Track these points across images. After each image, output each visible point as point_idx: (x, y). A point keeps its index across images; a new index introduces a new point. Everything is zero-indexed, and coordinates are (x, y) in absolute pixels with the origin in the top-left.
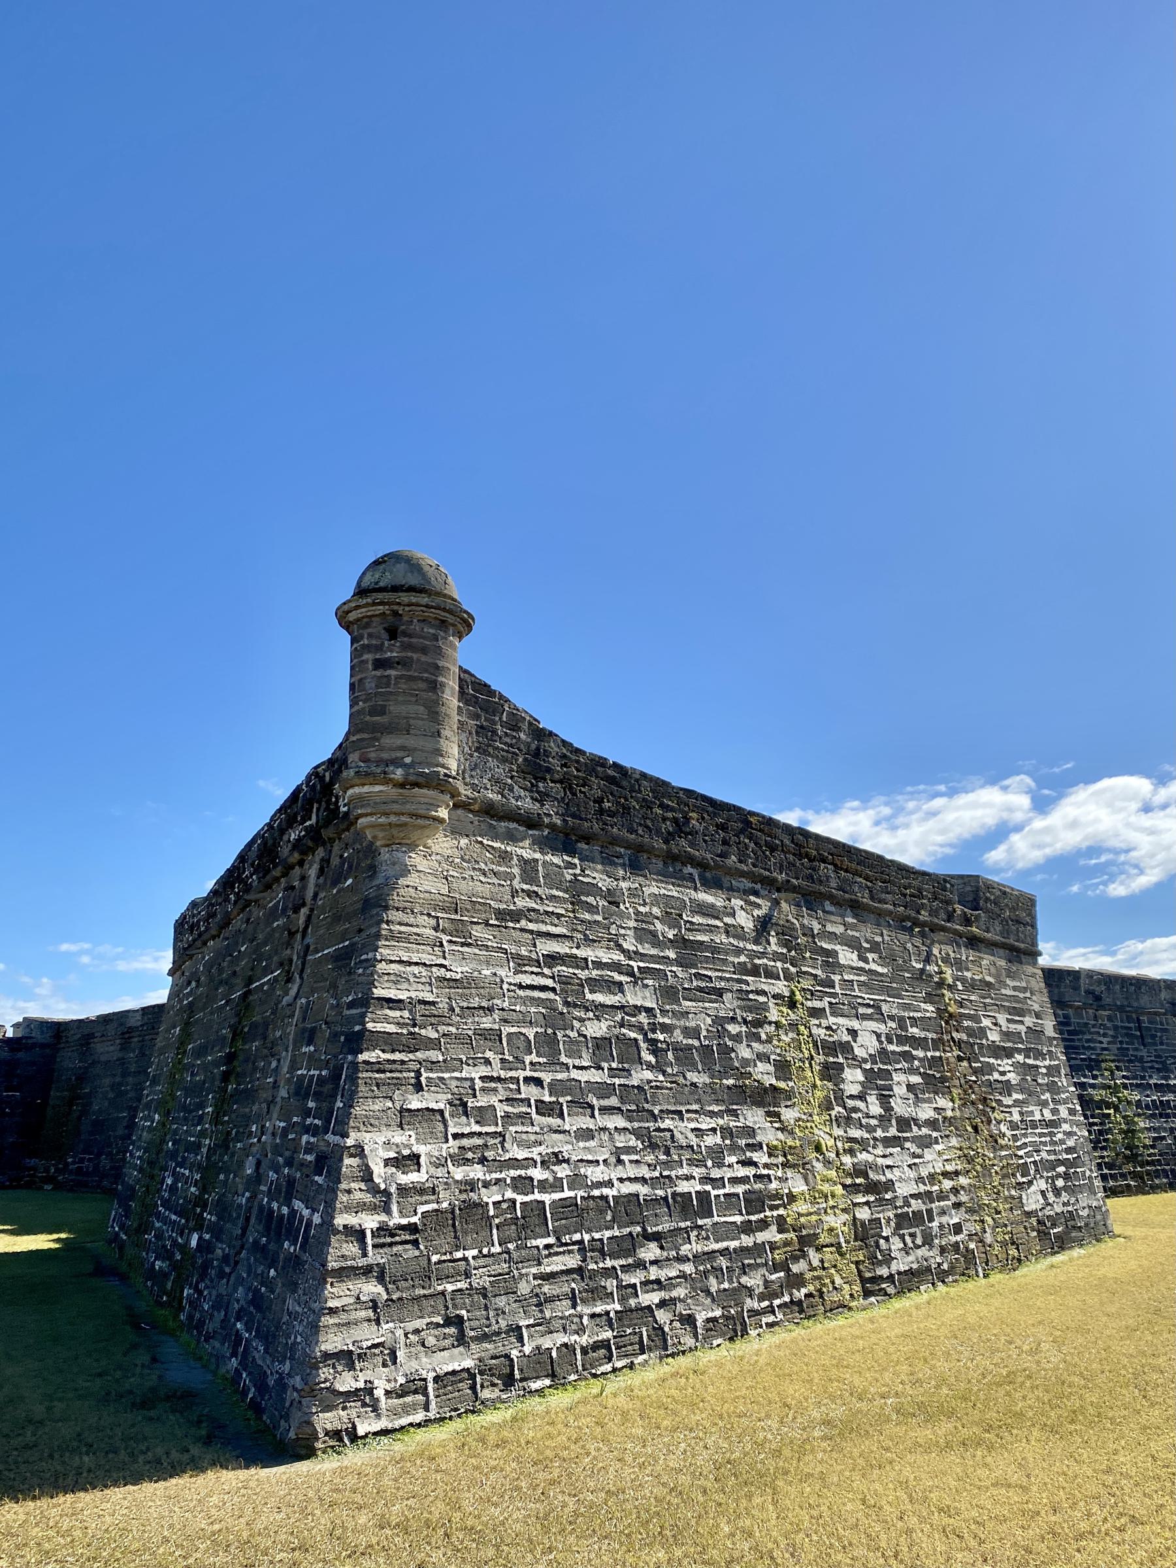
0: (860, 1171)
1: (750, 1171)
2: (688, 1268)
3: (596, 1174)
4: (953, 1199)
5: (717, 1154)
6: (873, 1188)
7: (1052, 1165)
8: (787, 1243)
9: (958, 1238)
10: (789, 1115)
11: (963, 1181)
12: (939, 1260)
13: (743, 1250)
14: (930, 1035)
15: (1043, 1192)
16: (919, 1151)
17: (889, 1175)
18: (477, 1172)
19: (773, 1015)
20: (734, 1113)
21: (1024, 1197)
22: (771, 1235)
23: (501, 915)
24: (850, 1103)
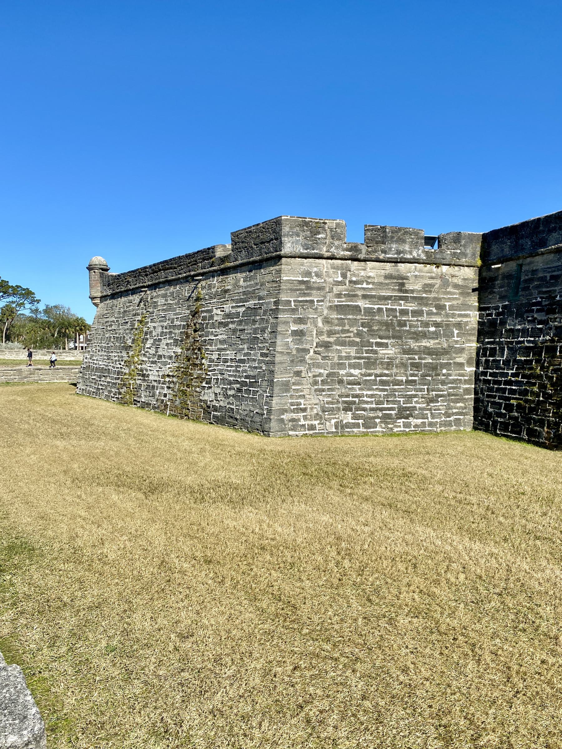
0: (142, 370)
1: (119, 366)
2: (106, 384)
3: (100, 363)
4: (167, 385)
5: (116, 361)
6: (143, 375)
7: (230, 383)
8: (121, 384)
9: (164, 398)
10: (131, 353)
11: (175, 380)
12: (155, 403)
13: (113, 383)
14: (182, 323)
15: (216, 394)
16: (162, 366)
17: (150, 373)
18: (91, 361)
19: (136, 327)
20: (121, 352)
21: (203, 393)
22: (119, 381)
23: (103, 315)
24: (146, 350)
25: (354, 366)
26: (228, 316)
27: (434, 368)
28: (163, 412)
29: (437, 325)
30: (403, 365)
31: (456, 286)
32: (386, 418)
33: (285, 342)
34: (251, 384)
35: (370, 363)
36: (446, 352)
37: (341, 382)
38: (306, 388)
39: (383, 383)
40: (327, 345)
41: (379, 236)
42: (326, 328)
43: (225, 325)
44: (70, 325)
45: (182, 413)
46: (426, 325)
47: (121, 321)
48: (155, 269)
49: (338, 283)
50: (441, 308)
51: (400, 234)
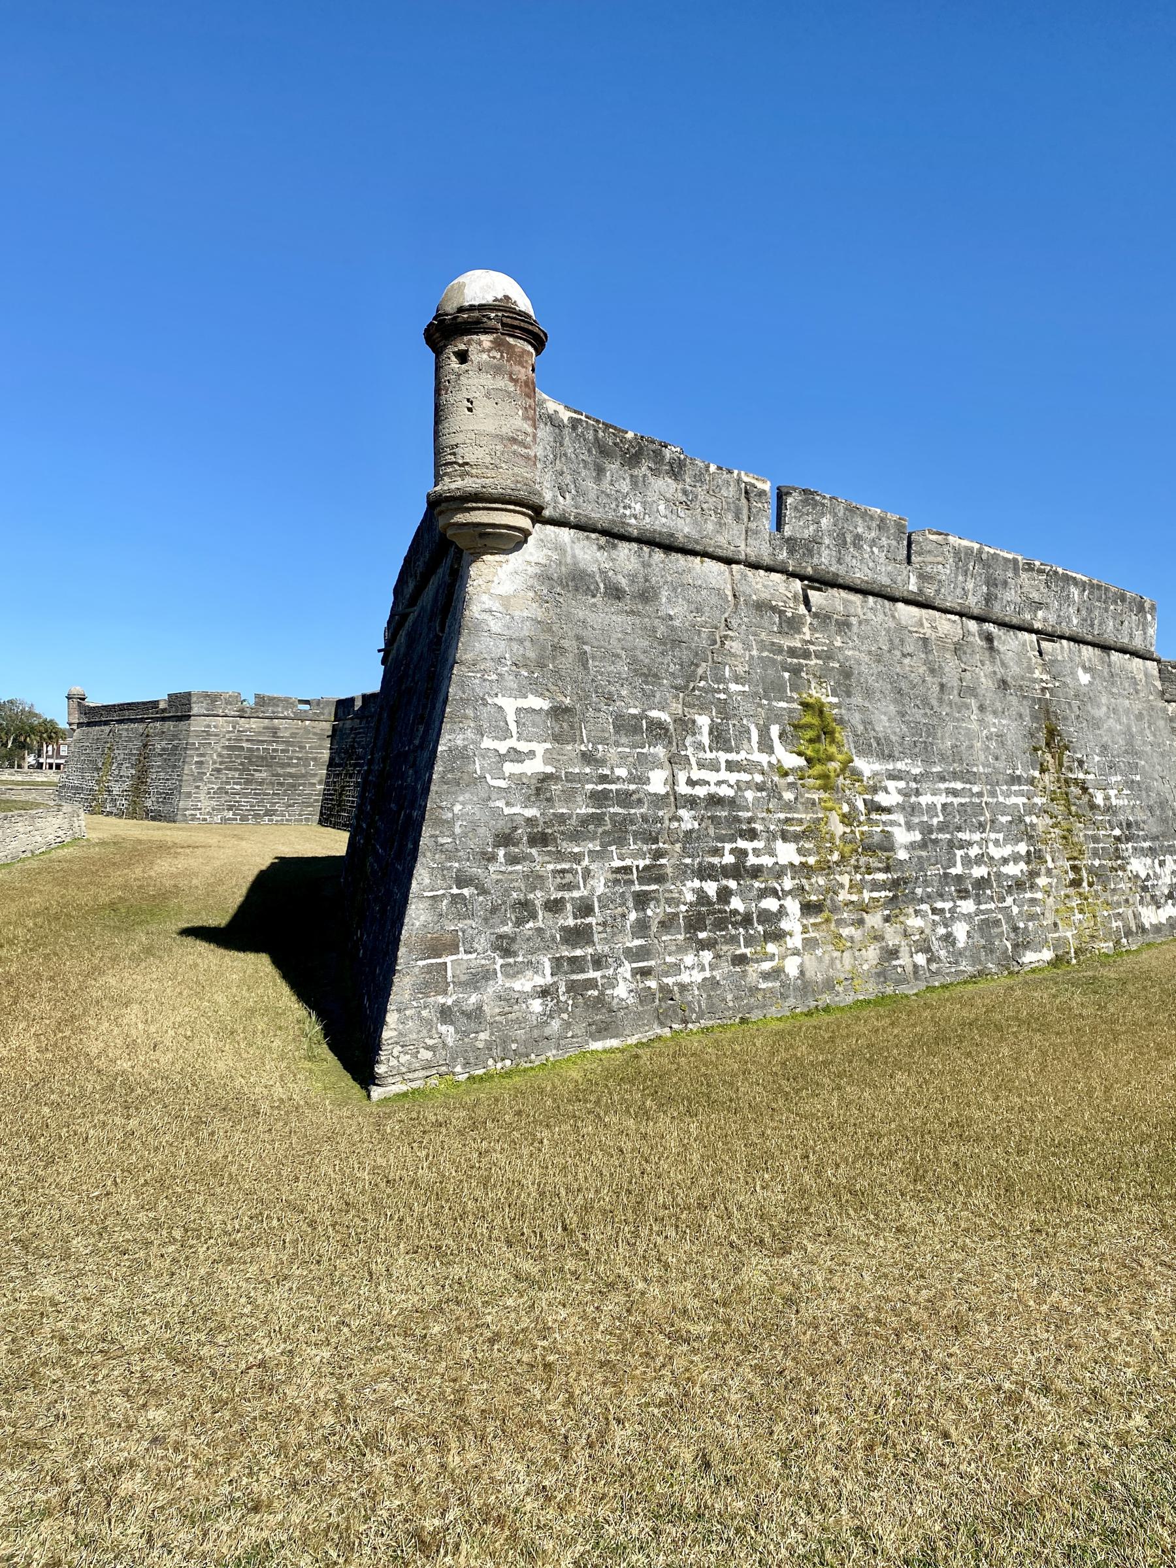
25: (237, 784)
26: (163, 749)
27: (293, 785)
28: (121, 817)
29: (298, 758)
30: (272, 784)
31: (315, 734)
32: (256, 816)
33: (190, 768)
34: (172, 794)
35: (248, 782)
36: (303, 776)
37: (227, 793)
38: (202, 796)
39: (255, 794)
40: (218, 770)
41: (261, 701)
42: (219, 760)
43: (161, 755)
44: (33, 730)
45: (132, 815)
46: (291, 758)
47: (95, 746)
48: (123, 707)
49: (229, 732)
50: (302, 748)
51: (274, 701)
